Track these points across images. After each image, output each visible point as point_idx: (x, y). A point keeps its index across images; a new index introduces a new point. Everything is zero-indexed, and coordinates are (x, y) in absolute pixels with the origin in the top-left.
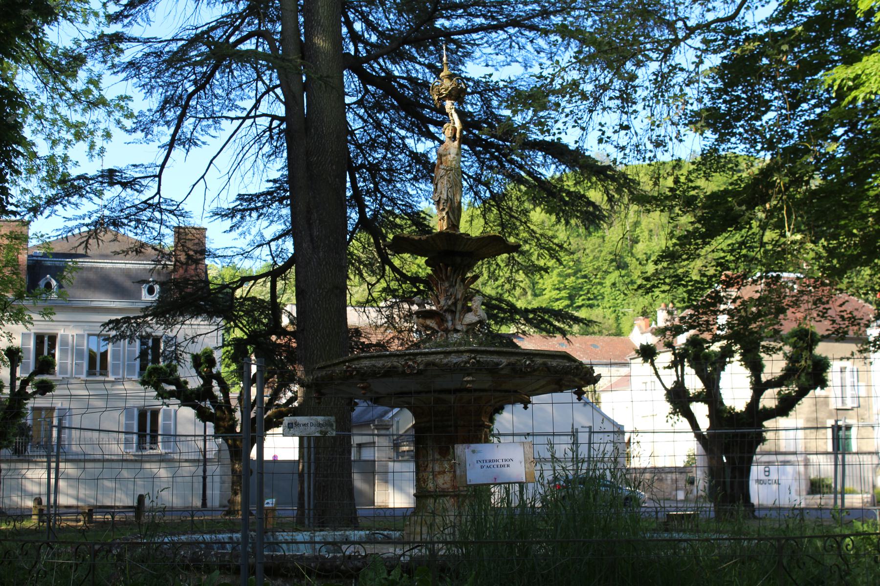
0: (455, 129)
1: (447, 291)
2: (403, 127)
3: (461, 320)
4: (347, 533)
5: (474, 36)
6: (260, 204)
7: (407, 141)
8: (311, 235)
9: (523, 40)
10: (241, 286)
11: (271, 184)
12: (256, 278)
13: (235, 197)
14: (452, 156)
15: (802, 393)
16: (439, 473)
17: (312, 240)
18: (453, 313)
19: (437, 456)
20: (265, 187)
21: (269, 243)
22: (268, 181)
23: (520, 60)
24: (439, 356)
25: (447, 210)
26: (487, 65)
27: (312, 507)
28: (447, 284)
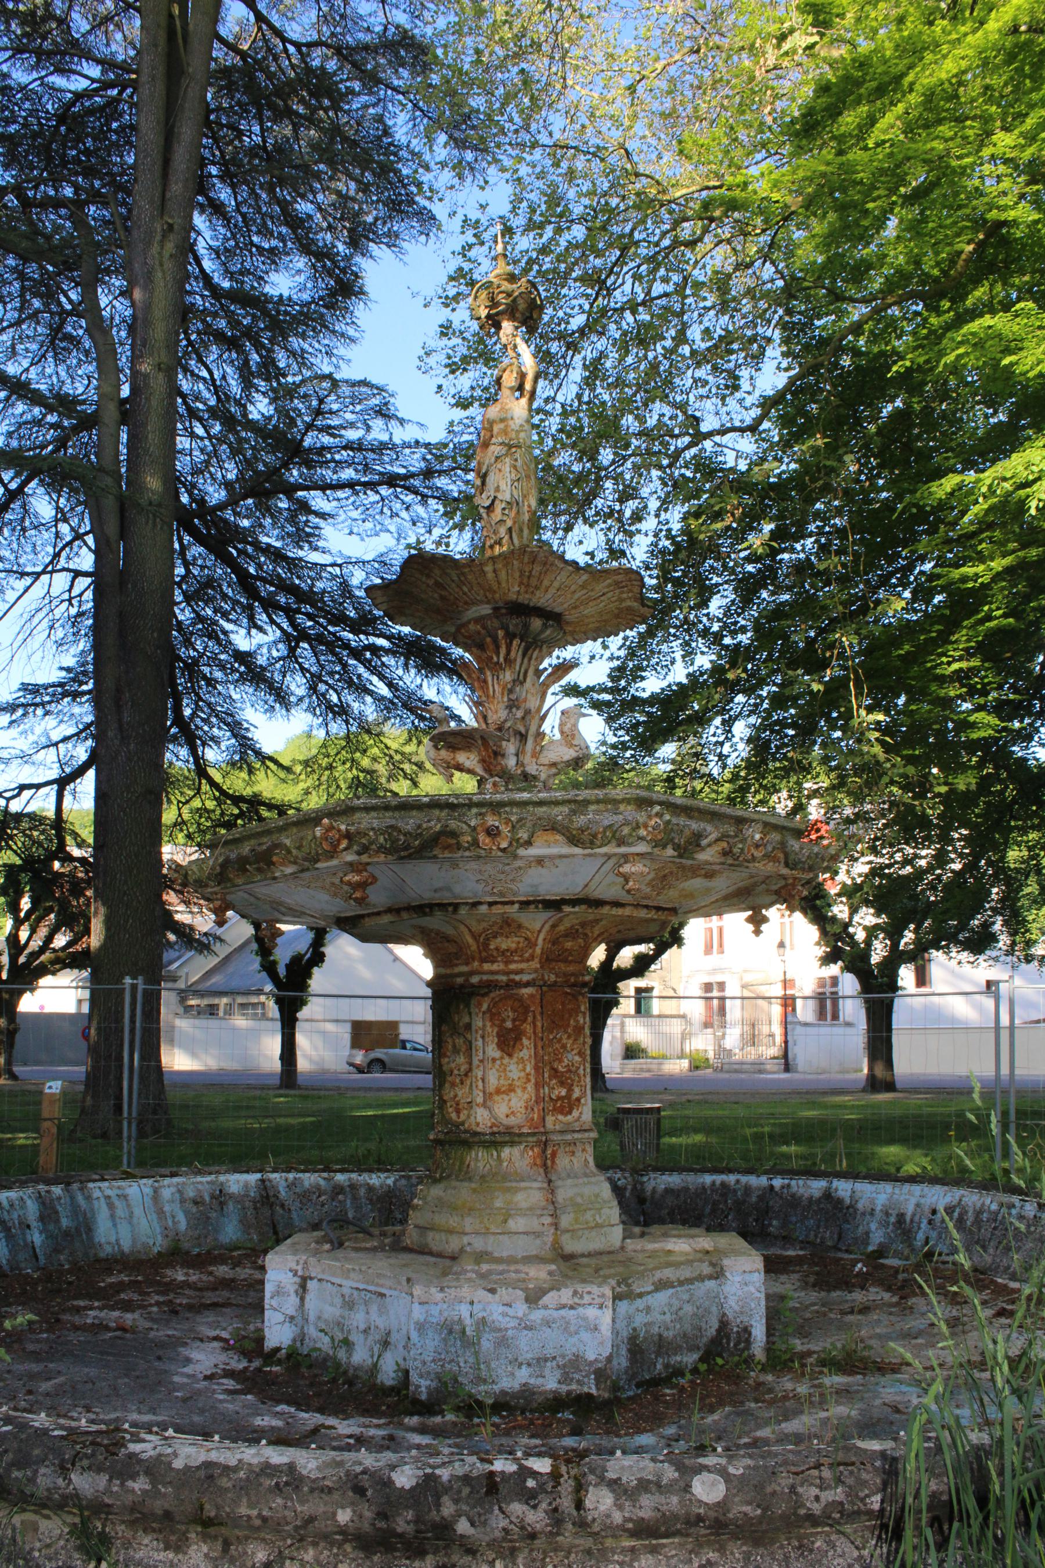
0: (522, 376)
1: (511, 691)
2: (229, 620)
3: (535, 755)
4: (222, 1178)
5: (340, 494)
6: (47, 698)
7: (232, 636)
8: (120, 721)
9: (397, 506)
10: (18, 795)
11: (64, 674)
12: (38, 787)
13: (16, 685)
14: (518, 422)
15: (660, 951)
16: (498, 1092)
17: (121, 728)
18: (523, 737)
19: (493, 1051)
20: (56, 676)
21: (56, 744)
22: (61, 668)
23: (393, 528)
24: (556, 810)
25: (509, 523)
26: (351, 533)
27: (134, 1114)
28: (508, 676)
